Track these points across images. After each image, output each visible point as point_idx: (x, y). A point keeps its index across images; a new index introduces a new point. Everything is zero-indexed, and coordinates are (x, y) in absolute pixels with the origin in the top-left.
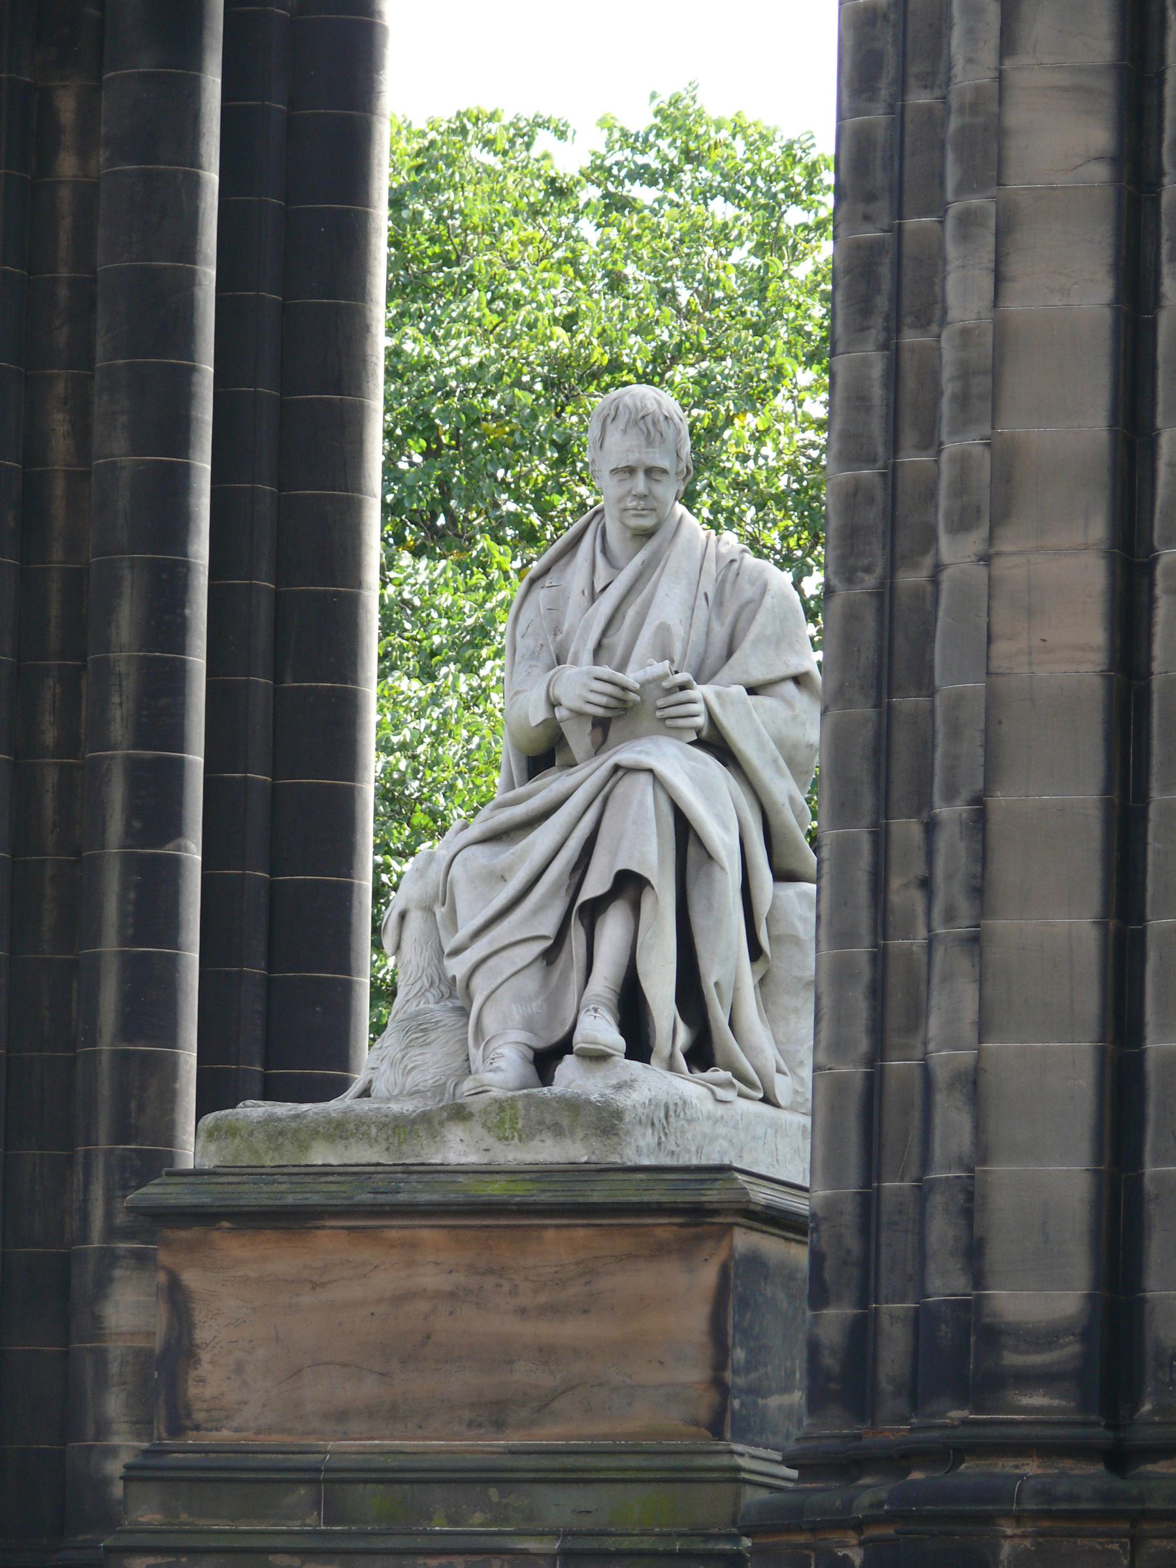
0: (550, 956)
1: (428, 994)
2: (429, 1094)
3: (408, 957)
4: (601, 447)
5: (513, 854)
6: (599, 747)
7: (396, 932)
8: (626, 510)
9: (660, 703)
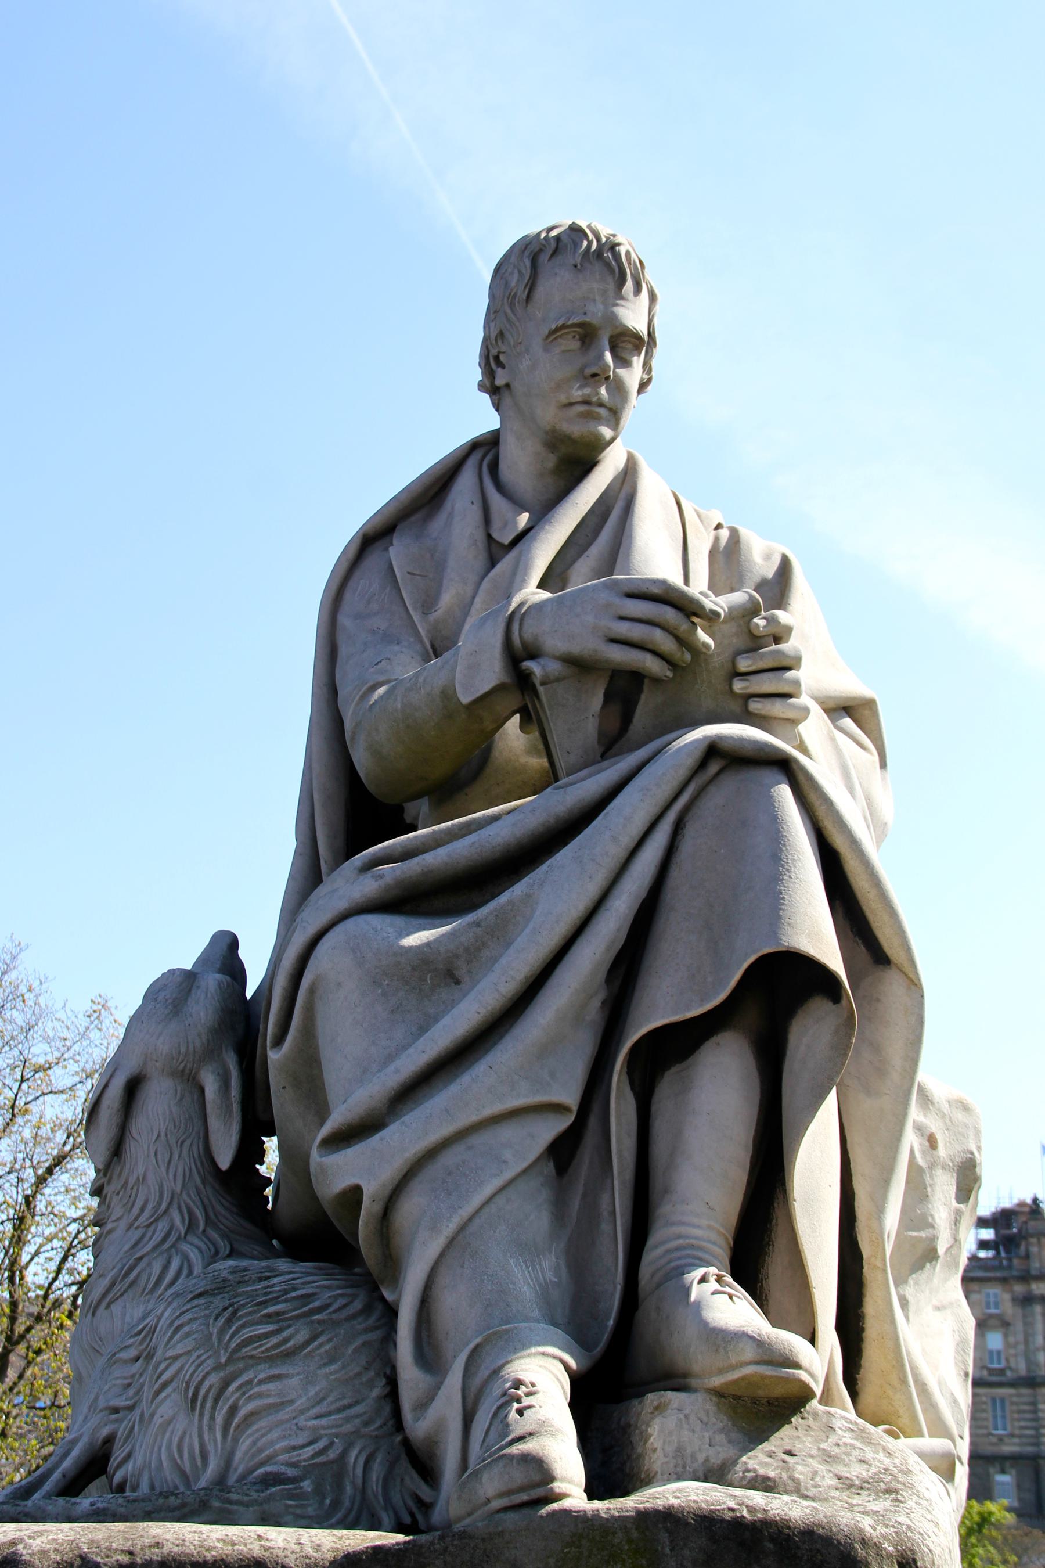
0: (562, 1153)
1: (185, 1247)
2: (307, 1485)
3: (141, 1170)
4: (529, 297)
5: (478, 924)
6: (610, 745)
7: (116, 1120)
8: (571, 404)
9: (744, 664)
